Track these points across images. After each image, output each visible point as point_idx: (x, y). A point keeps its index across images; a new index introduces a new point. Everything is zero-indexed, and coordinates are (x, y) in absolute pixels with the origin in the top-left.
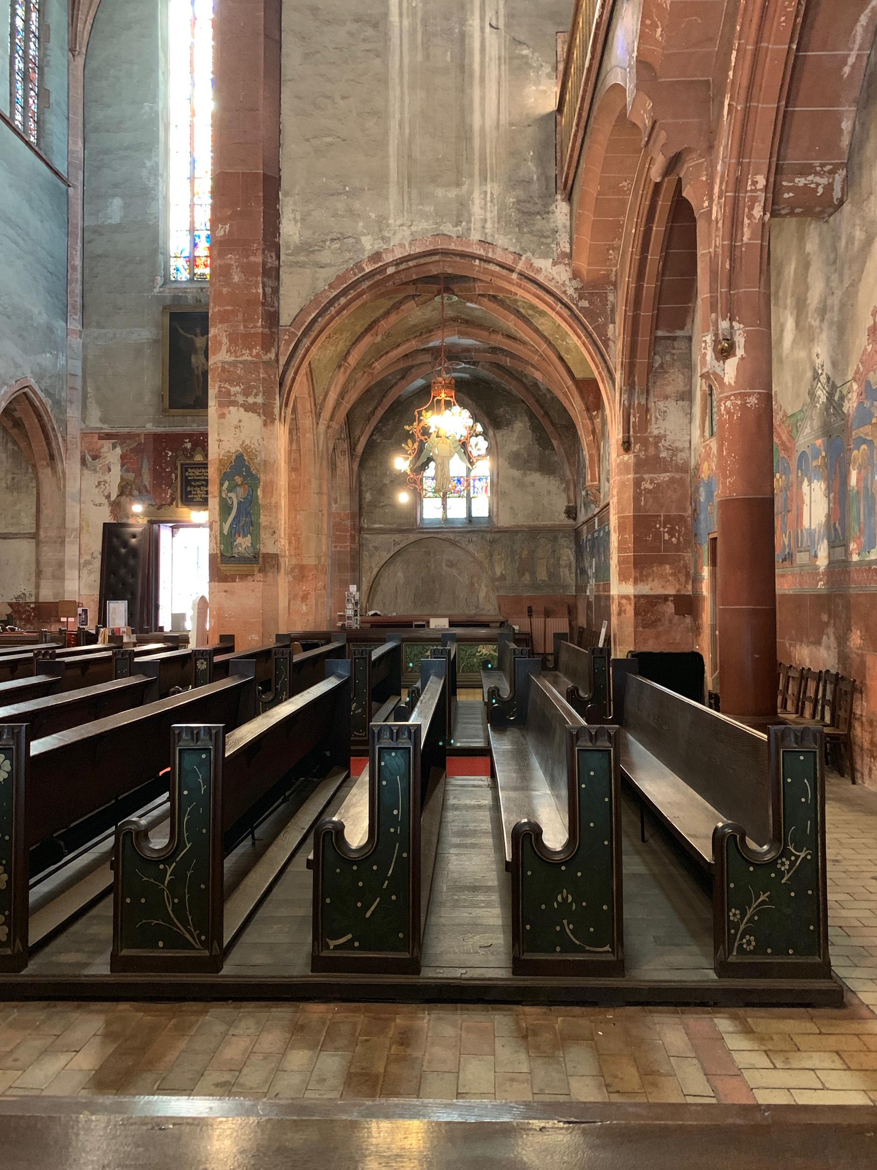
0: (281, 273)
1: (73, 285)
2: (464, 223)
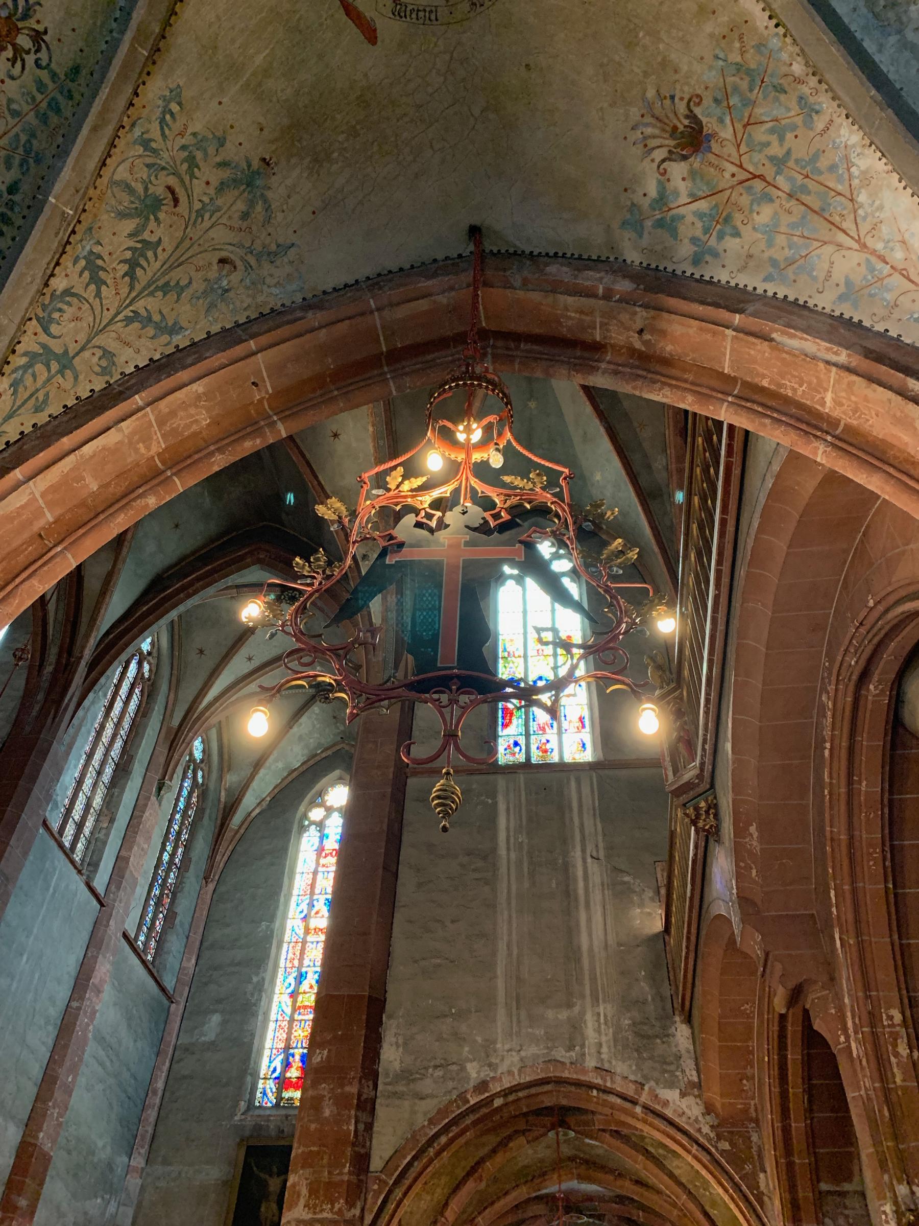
0: (377, 1107)
1: (149, 1112)
2: (577, 1048)
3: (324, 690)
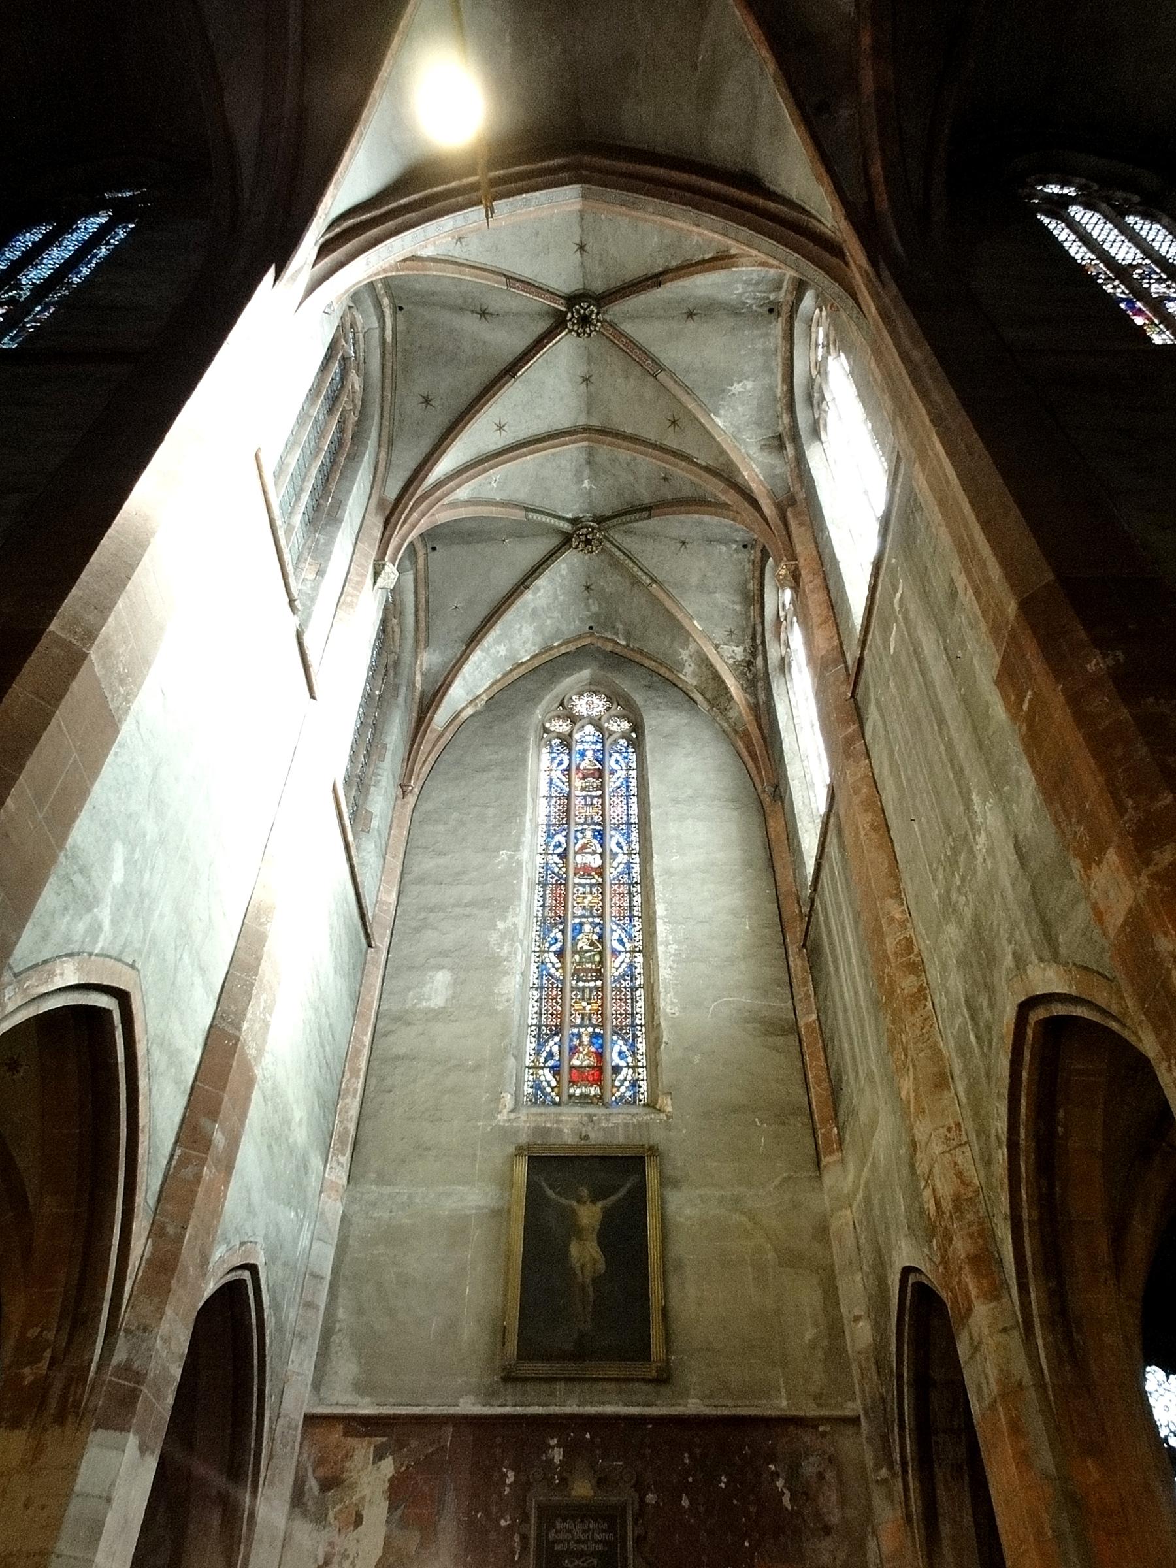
1: (348, 1100)
3: (587, 527)
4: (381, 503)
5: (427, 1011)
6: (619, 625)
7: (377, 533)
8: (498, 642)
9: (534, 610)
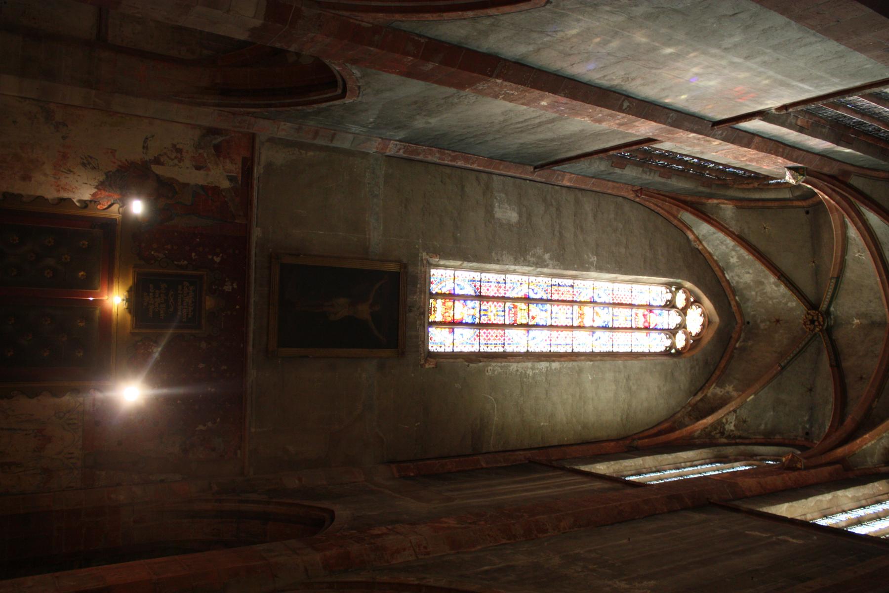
1: (437, 155)
3: (823, 321)
4: (847, 174)
5: (492, 206)
6: (750, 343)
7: (826, 170)
8: (740, 257)
9: (762, 283)
